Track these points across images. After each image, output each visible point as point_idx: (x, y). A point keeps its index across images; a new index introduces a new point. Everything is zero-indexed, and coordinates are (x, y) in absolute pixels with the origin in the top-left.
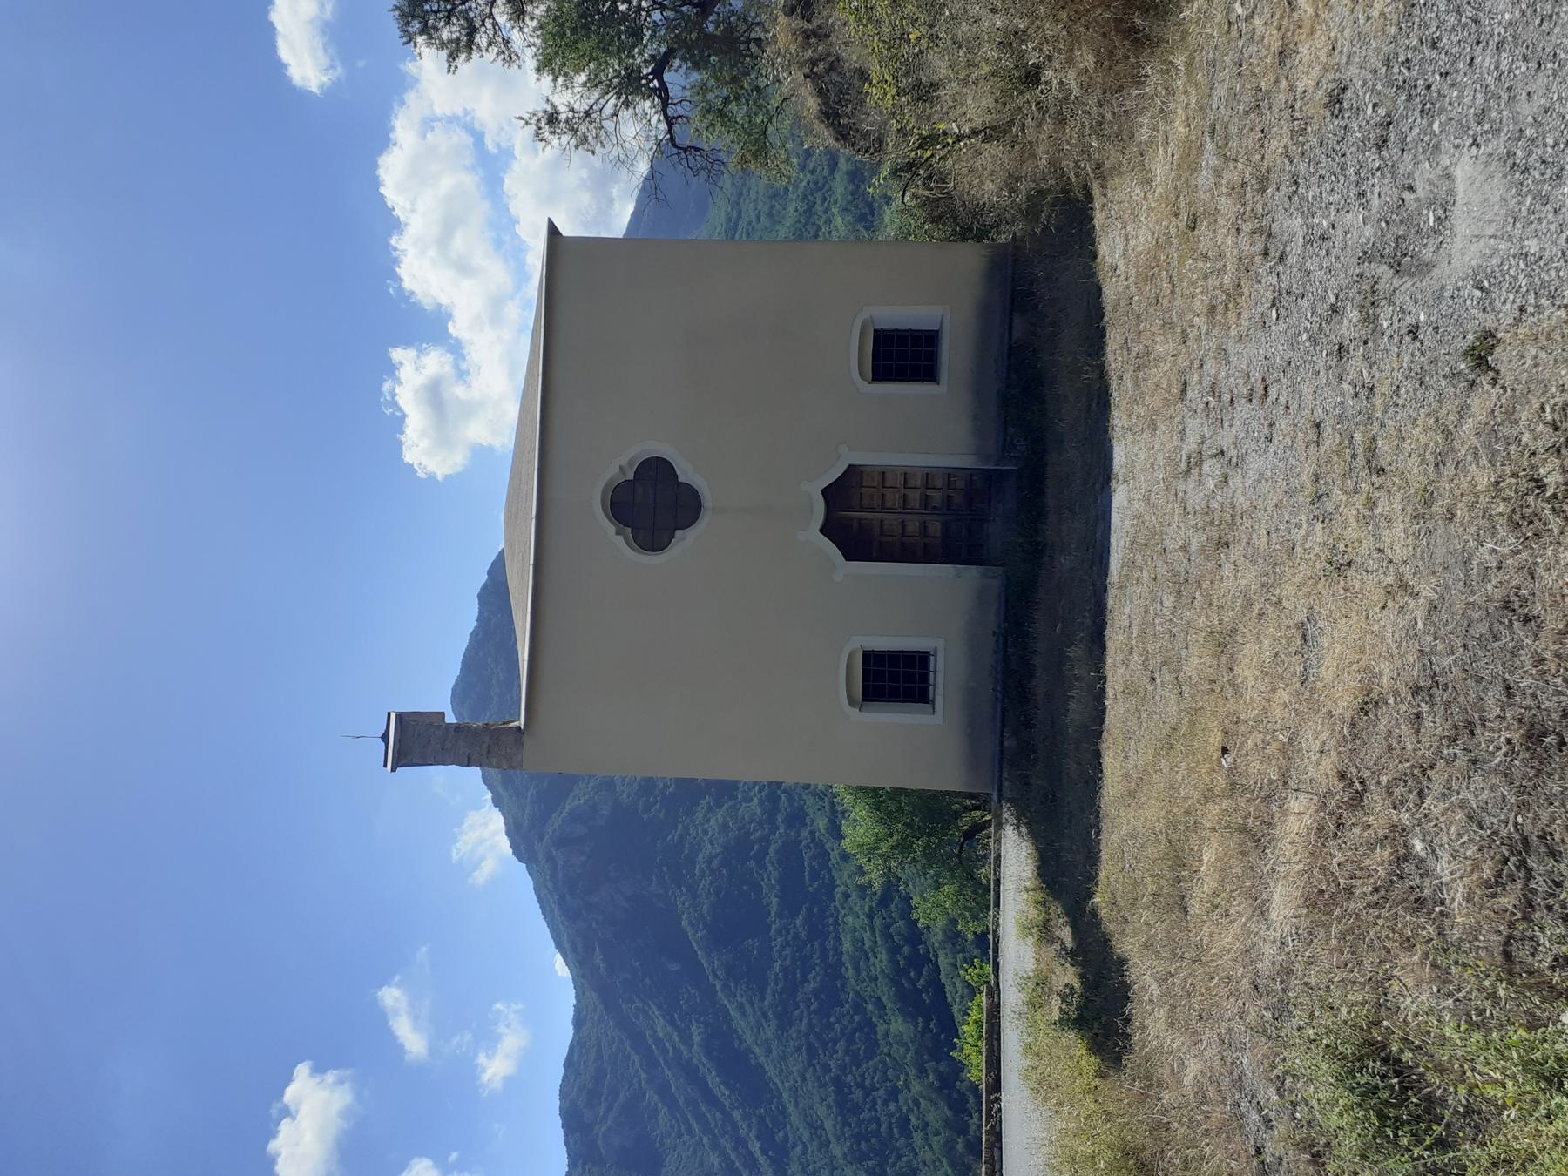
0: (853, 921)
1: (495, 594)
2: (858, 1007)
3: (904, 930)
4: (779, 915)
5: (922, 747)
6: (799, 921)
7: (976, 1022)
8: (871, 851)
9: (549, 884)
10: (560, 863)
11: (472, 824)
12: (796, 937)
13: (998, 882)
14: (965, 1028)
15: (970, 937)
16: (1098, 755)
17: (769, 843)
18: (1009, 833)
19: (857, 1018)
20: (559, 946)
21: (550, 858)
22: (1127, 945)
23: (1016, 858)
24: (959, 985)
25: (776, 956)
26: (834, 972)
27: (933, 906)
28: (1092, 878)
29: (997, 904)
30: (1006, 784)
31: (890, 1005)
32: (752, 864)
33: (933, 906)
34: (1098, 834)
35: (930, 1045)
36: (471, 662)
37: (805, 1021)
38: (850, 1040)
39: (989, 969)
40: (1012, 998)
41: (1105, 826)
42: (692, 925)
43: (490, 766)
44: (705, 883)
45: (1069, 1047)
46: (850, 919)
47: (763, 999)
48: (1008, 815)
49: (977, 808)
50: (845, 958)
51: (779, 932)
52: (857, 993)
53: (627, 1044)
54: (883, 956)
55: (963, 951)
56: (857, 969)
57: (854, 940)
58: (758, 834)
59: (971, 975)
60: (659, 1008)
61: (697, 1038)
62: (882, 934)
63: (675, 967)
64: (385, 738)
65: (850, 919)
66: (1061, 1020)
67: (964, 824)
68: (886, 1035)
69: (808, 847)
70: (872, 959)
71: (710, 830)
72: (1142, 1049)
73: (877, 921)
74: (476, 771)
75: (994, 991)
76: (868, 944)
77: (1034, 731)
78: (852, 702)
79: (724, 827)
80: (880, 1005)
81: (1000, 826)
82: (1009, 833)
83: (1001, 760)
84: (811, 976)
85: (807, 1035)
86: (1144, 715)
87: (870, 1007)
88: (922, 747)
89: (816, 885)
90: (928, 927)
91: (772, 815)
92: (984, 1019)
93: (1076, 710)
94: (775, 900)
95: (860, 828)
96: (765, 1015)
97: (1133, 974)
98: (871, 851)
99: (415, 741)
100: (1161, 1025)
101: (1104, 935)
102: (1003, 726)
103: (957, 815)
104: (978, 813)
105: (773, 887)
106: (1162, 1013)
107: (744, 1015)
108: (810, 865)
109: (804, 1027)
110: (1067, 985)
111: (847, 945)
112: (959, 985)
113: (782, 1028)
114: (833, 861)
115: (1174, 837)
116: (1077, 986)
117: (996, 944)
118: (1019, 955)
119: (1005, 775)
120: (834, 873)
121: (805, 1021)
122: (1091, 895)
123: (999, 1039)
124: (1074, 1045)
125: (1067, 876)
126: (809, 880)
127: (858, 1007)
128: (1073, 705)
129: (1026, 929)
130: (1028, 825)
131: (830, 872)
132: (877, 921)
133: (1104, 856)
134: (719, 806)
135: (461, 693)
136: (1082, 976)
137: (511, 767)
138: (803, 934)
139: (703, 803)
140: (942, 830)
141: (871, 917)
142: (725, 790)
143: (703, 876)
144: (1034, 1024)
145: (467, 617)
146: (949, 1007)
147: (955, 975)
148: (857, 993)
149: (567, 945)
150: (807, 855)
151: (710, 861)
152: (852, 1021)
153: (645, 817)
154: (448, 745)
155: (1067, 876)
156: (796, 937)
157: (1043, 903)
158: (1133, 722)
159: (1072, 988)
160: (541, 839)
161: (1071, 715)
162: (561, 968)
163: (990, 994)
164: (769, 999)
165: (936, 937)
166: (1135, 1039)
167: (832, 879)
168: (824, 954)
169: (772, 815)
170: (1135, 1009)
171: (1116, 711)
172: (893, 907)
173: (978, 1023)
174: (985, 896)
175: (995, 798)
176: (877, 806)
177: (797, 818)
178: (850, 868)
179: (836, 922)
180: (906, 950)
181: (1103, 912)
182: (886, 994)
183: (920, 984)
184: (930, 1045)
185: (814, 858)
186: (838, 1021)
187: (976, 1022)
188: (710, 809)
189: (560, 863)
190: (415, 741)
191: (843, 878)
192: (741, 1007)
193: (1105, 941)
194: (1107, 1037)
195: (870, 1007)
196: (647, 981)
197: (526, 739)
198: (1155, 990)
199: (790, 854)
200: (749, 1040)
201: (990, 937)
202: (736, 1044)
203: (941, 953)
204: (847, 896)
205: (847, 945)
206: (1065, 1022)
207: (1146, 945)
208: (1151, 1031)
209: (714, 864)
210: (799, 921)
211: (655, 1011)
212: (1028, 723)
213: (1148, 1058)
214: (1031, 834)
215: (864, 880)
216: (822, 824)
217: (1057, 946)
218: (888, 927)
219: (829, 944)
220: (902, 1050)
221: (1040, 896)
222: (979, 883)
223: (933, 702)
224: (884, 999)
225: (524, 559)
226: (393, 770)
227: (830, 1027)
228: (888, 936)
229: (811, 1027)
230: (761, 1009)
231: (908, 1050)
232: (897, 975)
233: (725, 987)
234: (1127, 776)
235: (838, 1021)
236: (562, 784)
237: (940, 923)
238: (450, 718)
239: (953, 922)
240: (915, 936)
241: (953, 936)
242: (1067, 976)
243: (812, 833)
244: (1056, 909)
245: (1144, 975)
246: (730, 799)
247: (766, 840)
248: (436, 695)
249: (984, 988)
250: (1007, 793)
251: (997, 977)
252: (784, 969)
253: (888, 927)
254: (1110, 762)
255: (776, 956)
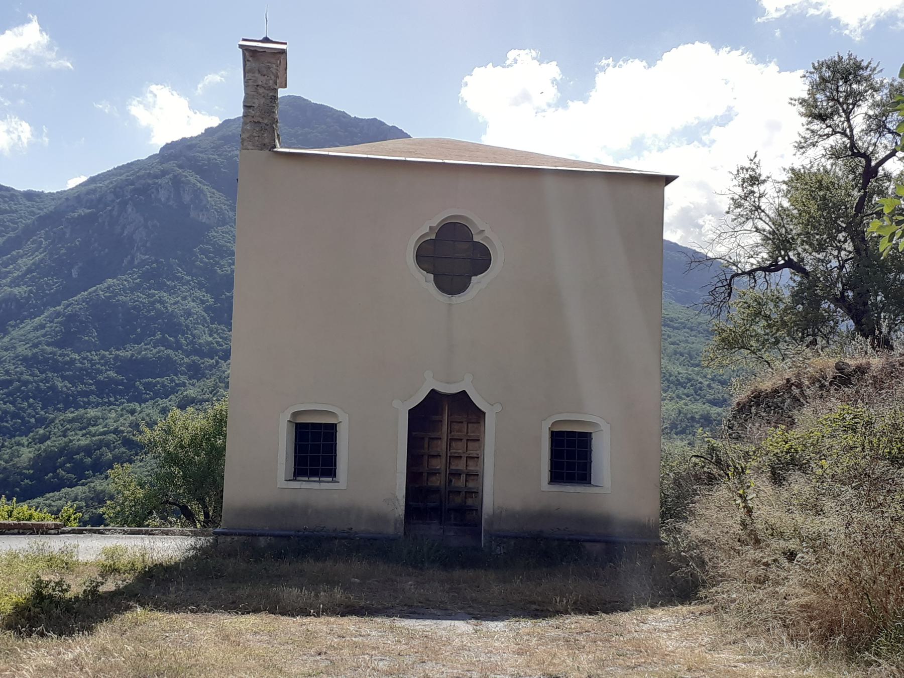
0: (113, 418)
1: (377, 131)
2: (41, 422)
3: (104, 459)
4: (117, 357)
5: (259, 473)
6: (112, 374)
7: (31, 515)
8: (168, 431)
9: (142, 172)
10: (160, 181)
11: (180, 109)
12: (100, 372)
13: (147, 533)
14: (25, 507)
15: (101, 511)
16: (256, 611)
17: (176, 350)
18: (189, 542)
19: (33, 420)
20: (92, 180)
21: (164, 173)
22: (104, 634)
23: (169, 546)
24: (59, 503)
25: (84, 354)
26: (70, 402)
27: (126, 481)
28: (157, 607)
29: (125, 532)
30: (229, 539)
31: (43, 447)
32: (159, 336)
33: (126, 481)
34: (192, 611)
35: (11, 479)
36: (322, 111)
37: (31, 378)
38: (15, 416)
39: (75, 526)
40: (55, 544)
41: (199, 617)
42: (108, 288)
43: (245, 123)
44: (143, 299)
45: (17, 587)
46: (113, 415)
47: (48, 344)
48: (202, 541)
49: (206, 515)
50: (82, 411)
51: (103, 357)
52: (53, 421)
53: (12, 234)
54: (84, 442)
55: (87, 506)
56: (71, 421)
57: (97, 418)
58: (183, 341)
59: (68, 509)
60: (41, 261)
61: (16, 290)
62: (101, 441)
63: (75, 273)
64: (266, 40)
65: (113, 415)
66: (41, 581)
67: (194, 506)
68: (19, 444)
69: (172, 381)
70: (80, 433)
71: (186, 302)
72: (19, 646)
73: (111, 437)
74: (239, 112)
75: (58, 530)
76: (93, 429)
77: (262, 563)
78: (295, 414)
79: (188, 314)
80: (43, 439)
81: (195, 534)
82: (189, 542)
83: (248, 535)
84: (67, 383)
85: (19, 380)
86: (290, 647)
87: (41, 431)
88: (259, 473)
89: (141, 387)
90: (107, 477)
91: (198, 352)
92: (33, 522)
93: (292, 594)
94: (129, 354)
95: (191, 422)
96: (35, 346)
97: (79, 638)
98: (168, 431)
99: (264, 65)
100: (41, 661)
101: (111, 616)
102: (276, 536)
103: (201, 500)
104: (202, 518)
105: (139, 353)
106: (50, 662)
107: (36, 329)
108: (158, 382)
109: (25, 377)
110: (69, 586)
111: (92, 413)
112: (59, 503)
113: (25, 359)
114: (160, 402)
115: (194, 670)
116: (68, 595)
117: (95, 532)
118: (90, 549)
119: (236, 538)
120: (150, 402)
121: (31, 378)
122: (142, 605)
123: (19, 534)
124: (23, 591)
125: (155, 587)
126: (136, 383)
127: (41, 422)
128: (295, 591)
129: (111, 554)
130: (195, 557)
131: (152, 399)
132: (111, 437)
133: (174, 616)
134: (206, 310)
135: (298, 103)
136: (77, 598)
137: (243, 140)
138: (101, 377)
139: (208, 297)
140: (191, 484)
141: (116, 431)
142: (222, 314)
143: (148, 296)
144: (35, 560)
145: (358, 110)
146: (41, 494)
147: (65, 502)
148: (53, 421)
149: (92, 186)
150: (165, 380)
151: (161, 302)
152: (30, 416)
153: (196, 250)
154: (261, 91)
155: (155, 587)
156: (100, 372)
157: (133, 569)
158: (284, 638)
159: (66, 591)
160: (180, 167)
161: (287, 590)
162: (73, 183)
163: (57, 527)
164: (49, 349)
165: (99, 484)
166: (28, 640)
167: (146, 401)
168: (86, 394)
169: (198, 352)
170: (53, 640)
171: (293, 625)
172: (123, 449)
173: (30, 517)
174: (136, 521)
175: (218, 530)
176: (207, 437)
177: (196, 373)
178: (156, 416)
179: (110, 404)
180: (88, 460)
181: (128, 615)
182: (54, 443)
183: (60, 472)
184: (11, 479)
185: (163, 386)
186: (30, 405)
187: (31, 515)
188: (203, 302)
189: (160, 181)
190: (264, 65)
191: (149, 410)
192: (42, 326)
193: (106, 617)
194: (29, 619)
195: (41, 431)
196: (63, 251)
197: (265, 153)
198: (69, 656)
199: (166, 366)
200: (15, 333)
201: (102, 527)
202: (12, 323)
203: (86, 488)
204: (132, 412)
205: (92, 413)
206: (39, 585)
207: (104, 650)
208: (35, 653)
209: (158, 306)
210: (112, 374)
211: (39, 257)
212: (279, 556)
213: (13, 651)
214: (187, 560)
215: (143, 427)
216: (191, 392)
217: (100, 579)
218: (108, 445)
219: (93, 398)
220: (6, 457)
221: (139, 566)
222: (146, 518)
223: (295, 480)
224: (48, 442)
225: (410, 153)
226: (241, 46)
227: (26, 399)
228: (99, 445)
229: (26, 383)
230: (40, 343)
231: (6, 462)
232: (67, 452)
233: (58, 314)
234: (240, 633)
235: (30, 405)
236: (229, 186)
237: (111, 488)
238: (281, 93)
239: (111, 498)
240: (100, 468)
241: (99, 498)
242: (76, 587)
243: (184, 385)
244: (130, 578)
245: (79, 648)
246: (211, 318)
247: (178, 347)
248: (300, 84)
249: (58, 522)
250: (221, 539)
251: (69, 532)
252: (73, 361)
253: (108, 445)
254: (249, 621)
255: (84, 354)
